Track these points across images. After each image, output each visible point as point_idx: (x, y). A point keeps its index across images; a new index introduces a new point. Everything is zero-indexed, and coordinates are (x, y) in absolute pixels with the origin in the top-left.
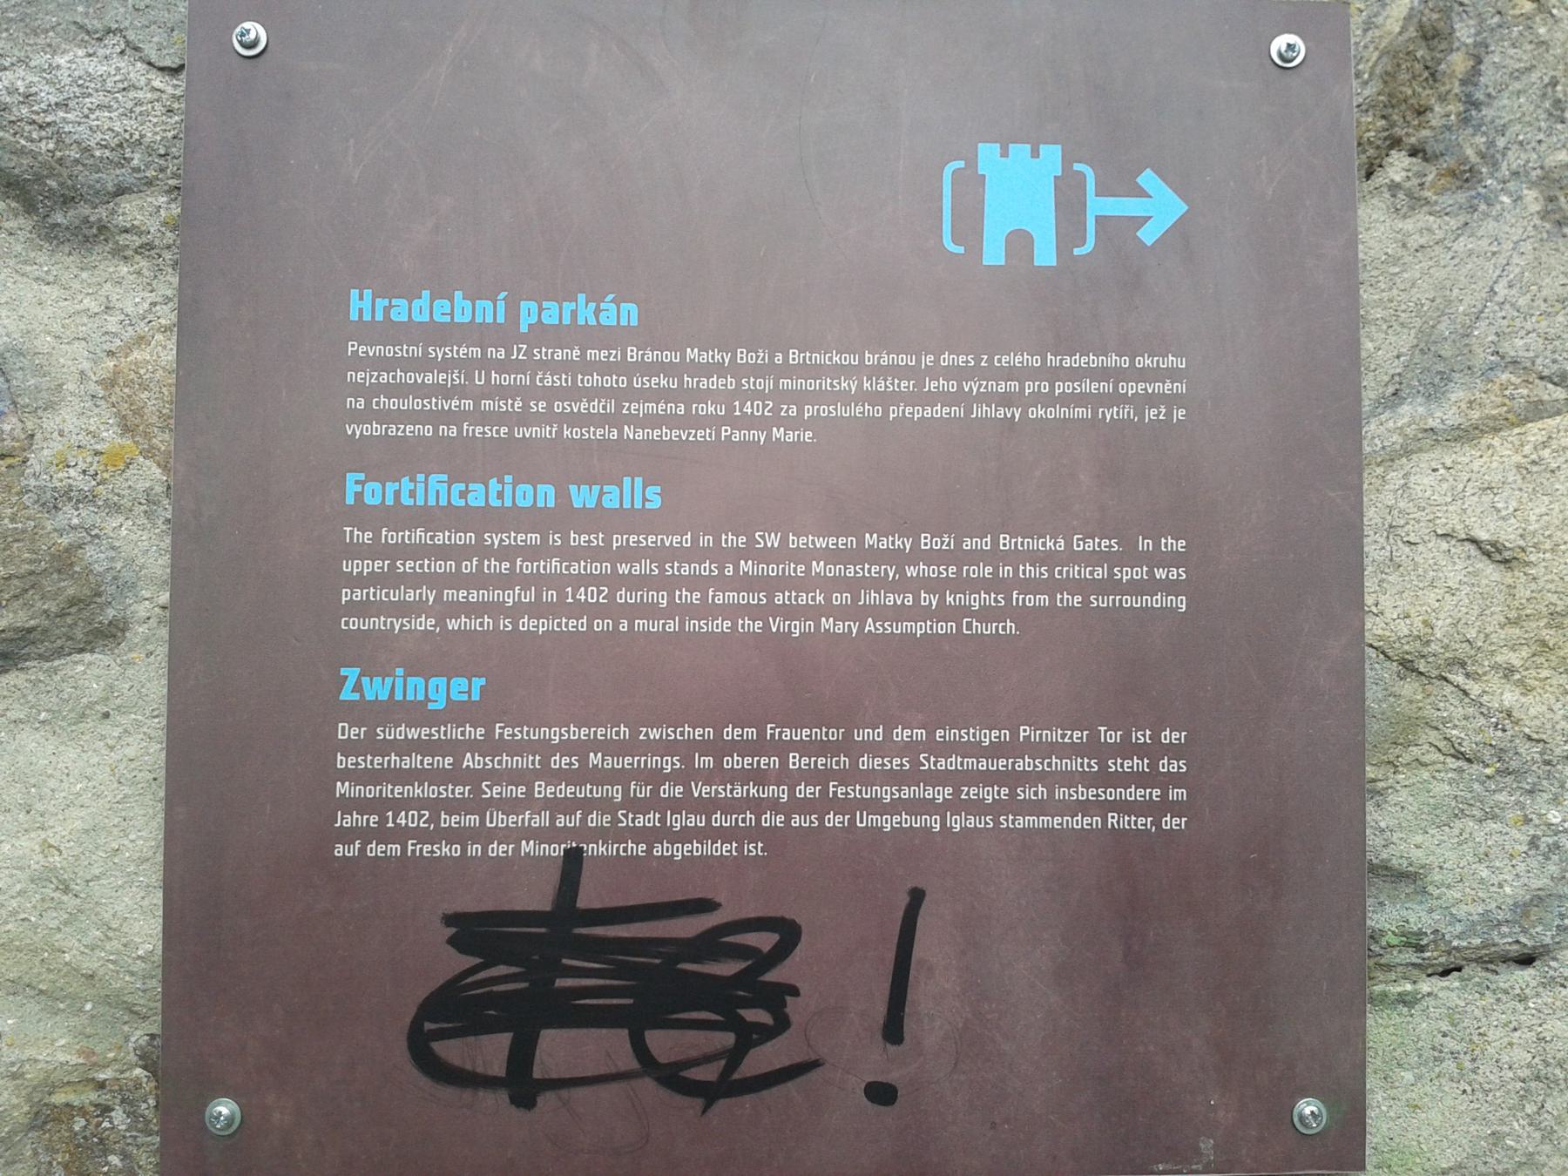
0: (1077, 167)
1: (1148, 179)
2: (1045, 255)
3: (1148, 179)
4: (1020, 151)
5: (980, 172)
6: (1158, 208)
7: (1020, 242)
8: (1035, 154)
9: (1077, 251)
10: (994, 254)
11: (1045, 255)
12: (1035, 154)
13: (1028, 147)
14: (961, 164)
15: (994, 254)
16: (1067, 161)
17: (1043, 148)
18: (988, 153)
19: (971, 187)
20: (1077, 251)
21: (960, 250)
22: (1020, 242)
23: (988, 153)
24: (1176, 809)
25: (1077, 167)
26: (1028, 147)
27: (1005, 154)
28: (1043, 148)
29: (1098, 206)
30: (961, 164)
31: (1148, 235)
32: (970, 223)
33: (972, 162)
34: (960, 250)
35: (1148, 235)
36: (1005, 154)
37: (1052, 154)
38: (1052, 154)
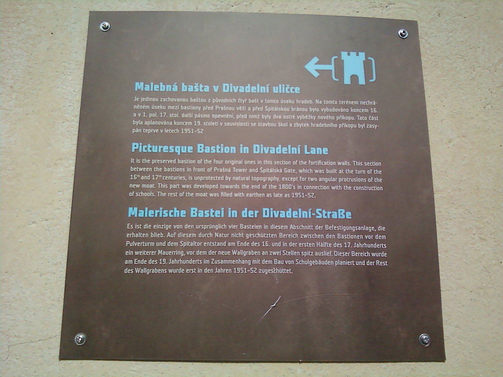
0: (369, 58)
2: (362, 81)
4: (353, 54)
5: (342, 59)
7: (354, 78)
8: (357, 55)
10: (347, 81)
11: (362, 81)
12: (357, 55)
13: (355, 53)
14: (336, 57)
15: (347, 81)
16: (366, 57)
17: (359, 53)
18: (344, 55)
21: (337, 80)
22: (354, 78)
23: (344, 55)
25: (369, 58)
27: (349, 54)
28: (359, 53)
30: (336, 57)
33: (340, 56)
34: (337, 80)
36: (349, 54)
37: (362, 55)
38: (362, 55)
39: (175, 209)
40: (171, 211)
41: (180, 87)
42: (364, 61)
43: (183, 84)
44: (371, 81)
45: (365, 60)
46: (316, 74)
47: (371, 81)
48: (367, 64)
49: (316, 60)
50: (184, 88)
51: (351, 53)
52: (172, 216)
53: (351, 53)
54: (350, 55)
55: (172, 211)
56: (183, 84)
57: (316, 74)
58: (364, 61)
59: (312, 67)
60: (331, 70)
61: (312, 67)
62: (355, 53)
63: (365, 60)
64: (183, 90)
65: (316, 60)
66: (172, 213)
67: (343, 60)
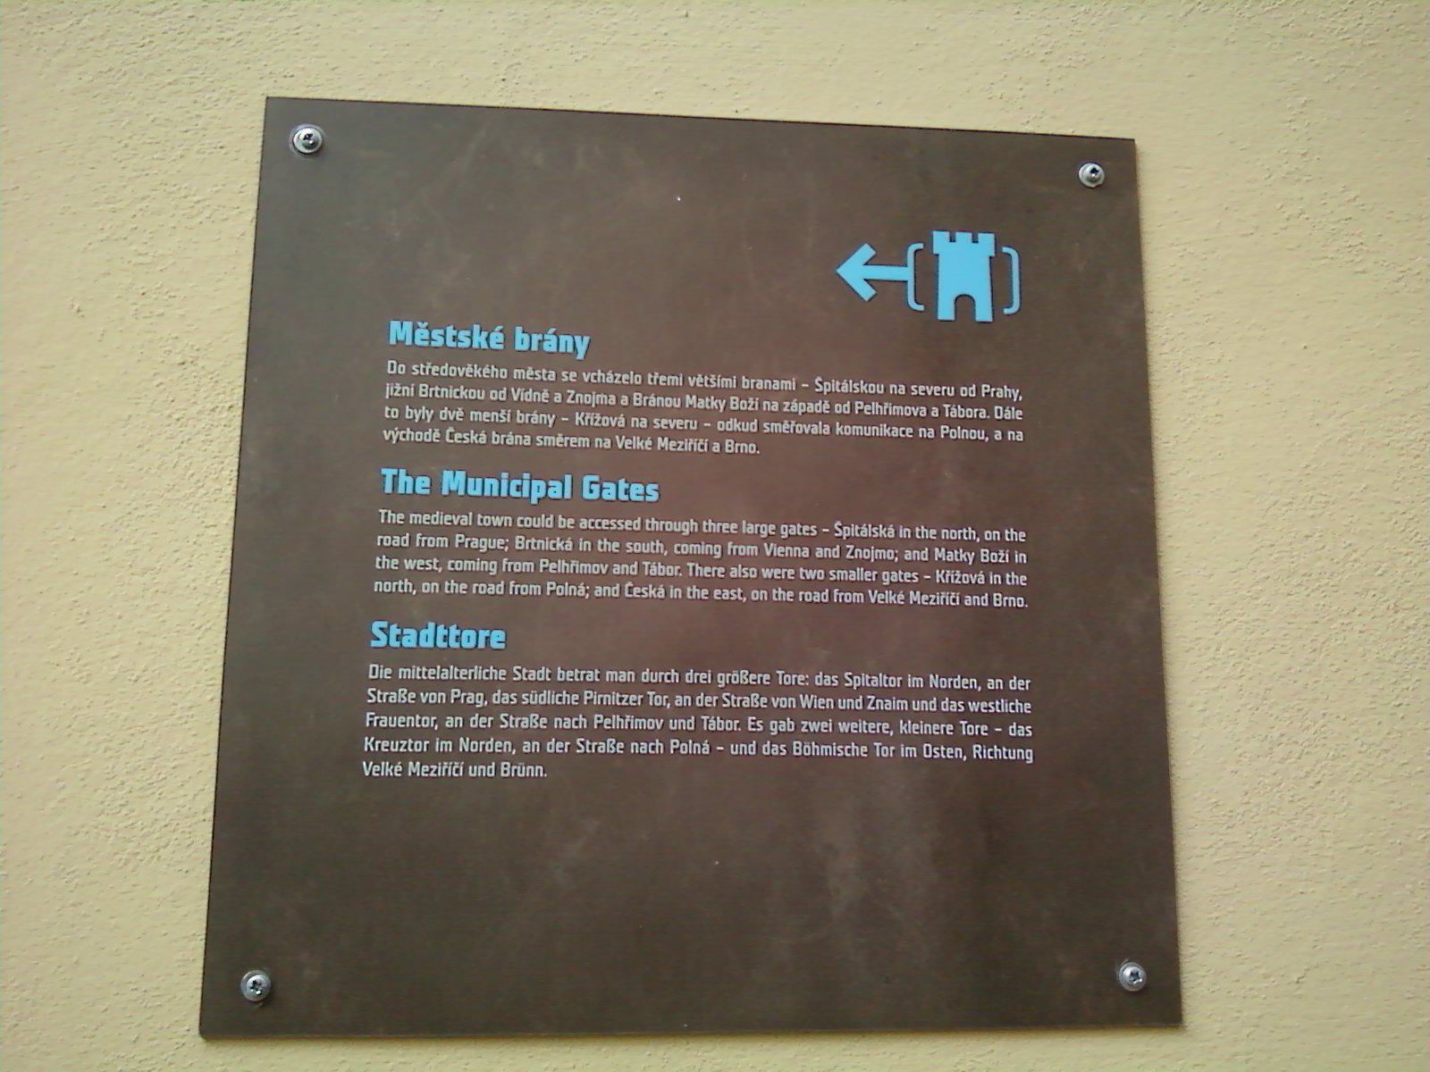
0: (1005, 250)
2: (983, 312)
4: (964, 238)
5: (935, 252)
7: (964, 303)
8: (975, 241)
9: (1006, 311)
10: (946, 311)
11: (983, 312)
12: (975, 241)
13: (970, 235)
14: (920, 246)
15: (946, 311)
17: (981, 236)
18: (940, 239)
21: (921, 308)
22: (964, 303)
23: (940, 239)
25: (1005, 250)
26: (970, 235)
27: (952, 240)
28: (981, 236)
30: (920, 246)
33: (929, 243)
34: (921, 308)
36: (952, 240)
37: (987, 240)
38: (987, 240)
41: (509, 339)
42: (991, 258)
43: (519, 330)
45: (993, 254)
46: (866, 292)
47: (1006, 311)
48: (998, 266)
49: (866, 252)
50: (521, 341)
51: (959, 235)
53: (959, 235)
54: (954, 241)
56: (519, 330)
57: (866, 292)
58: (991, 258)
59: (857, 271)
60: (906, 282)
61: (857, 271)
63: (993, 254)
64: (518, 347)
65: (866, 252)
67: (938, 255)
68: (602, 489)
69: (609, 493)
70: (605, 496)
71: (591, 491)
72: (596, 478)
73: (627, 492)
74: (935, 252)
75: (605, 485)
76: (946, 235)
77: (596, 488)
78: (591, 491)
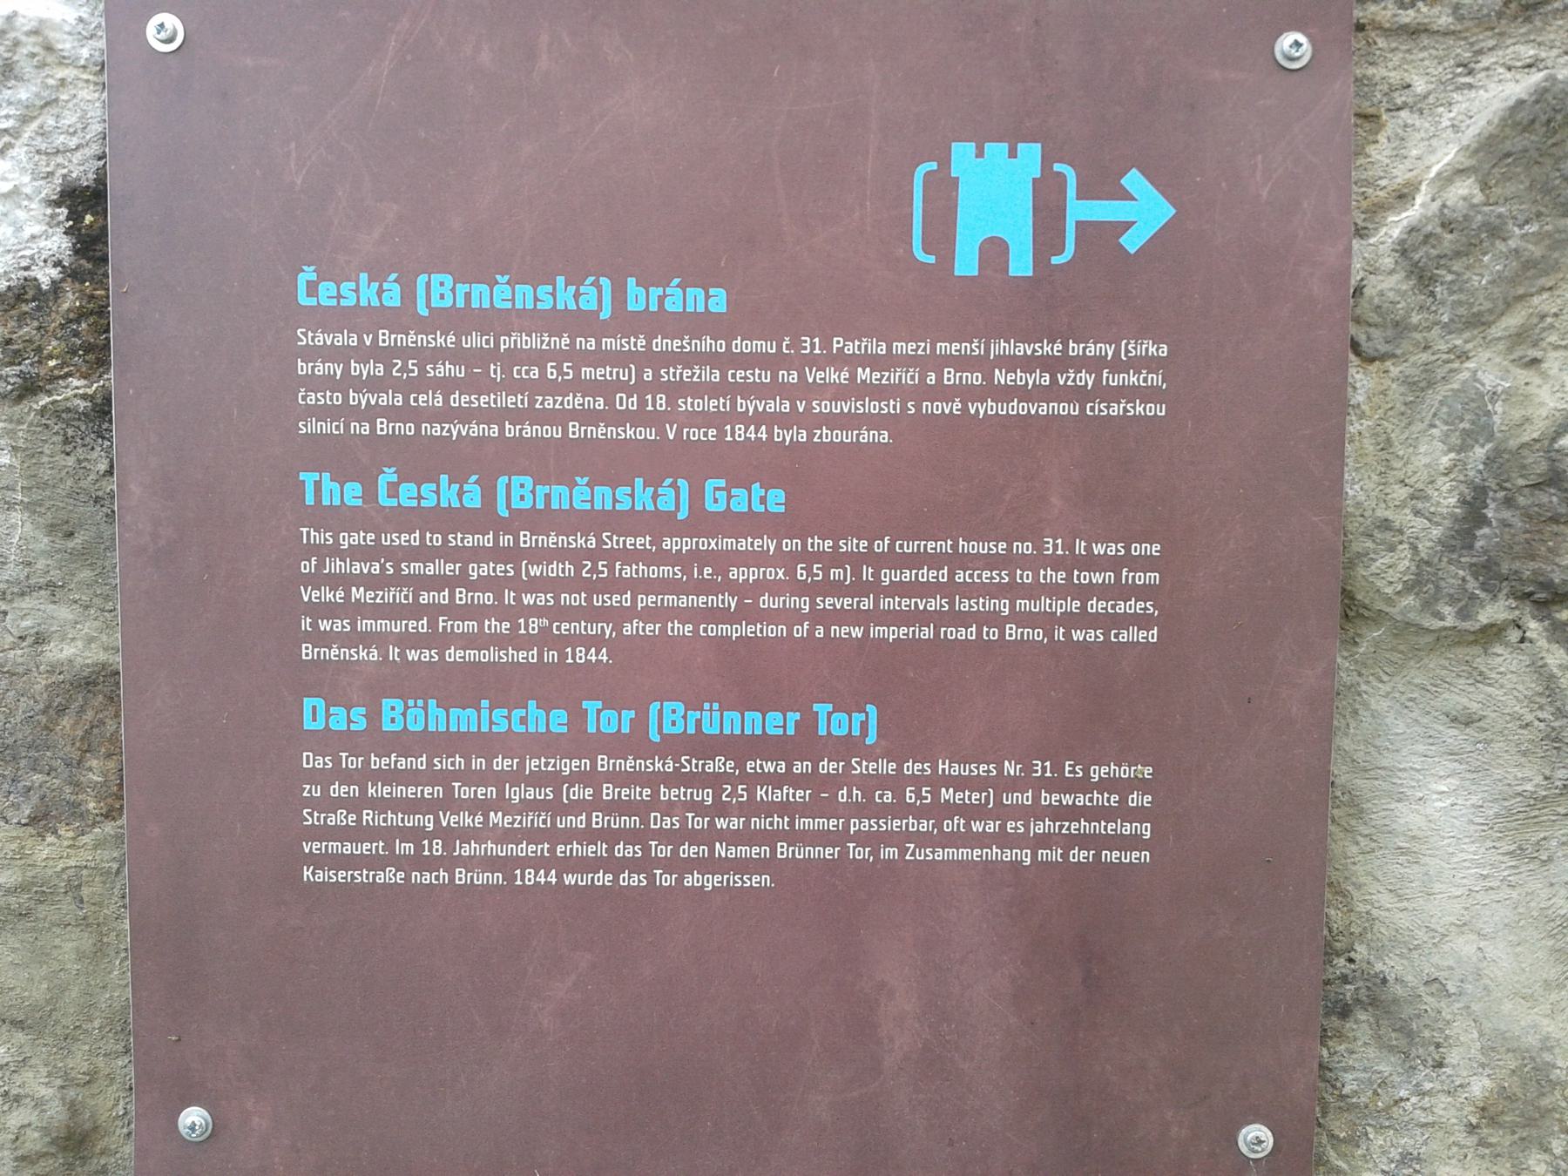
0: (1057, 167)
1: (1134, 180)
2: (1021, 264)
3: (1134, 180)
4: (997, 150)
5: (953, 175)
6: (1144, 211)
7: (995, 250)
8: (1013, 154)
10: (966, 264)
11: (1021, 264)
12: (1013, 154)
13: (1004, 147)
14: (933, 166)
15: (966, 264)
17: (1021, 146)
18: (962, 152)
19: (944, 190)
20: (1055, 260)
21: (931, 259)
22: (995, 250)
23: (962, 152)
24: (314, 776)
25: (1057, 167)
27: (980, 153)
28: (1021, 146)
29: (1079, 210)
30: (933, 166)
31: (1132, 242)
32: (942, 232)
33: (945, 162)
34: (931, 259)
35: (1132, 242)
36: (980, 153)
37: (1031, 153)
38: (1031, 153)
39: (532, 704)
40: (518, 713)
42: (1034, 180)
44: (1055, 260)
51: (990, 147)
52: (522, 729)
53: (990, 147)
55: (522, 712)
58: (1034, 180)
62: (1004, 147)
66: (524, 721)
68: (729, 497)
69: (740, 503)
70: (735, 508)
71: (716, 501)
72: (722, 483)
73: (763, 500)
74: (953, 175)
75: (734, 491)
76: (971, 147)
77: (722, 495)
78: (716, 501)
